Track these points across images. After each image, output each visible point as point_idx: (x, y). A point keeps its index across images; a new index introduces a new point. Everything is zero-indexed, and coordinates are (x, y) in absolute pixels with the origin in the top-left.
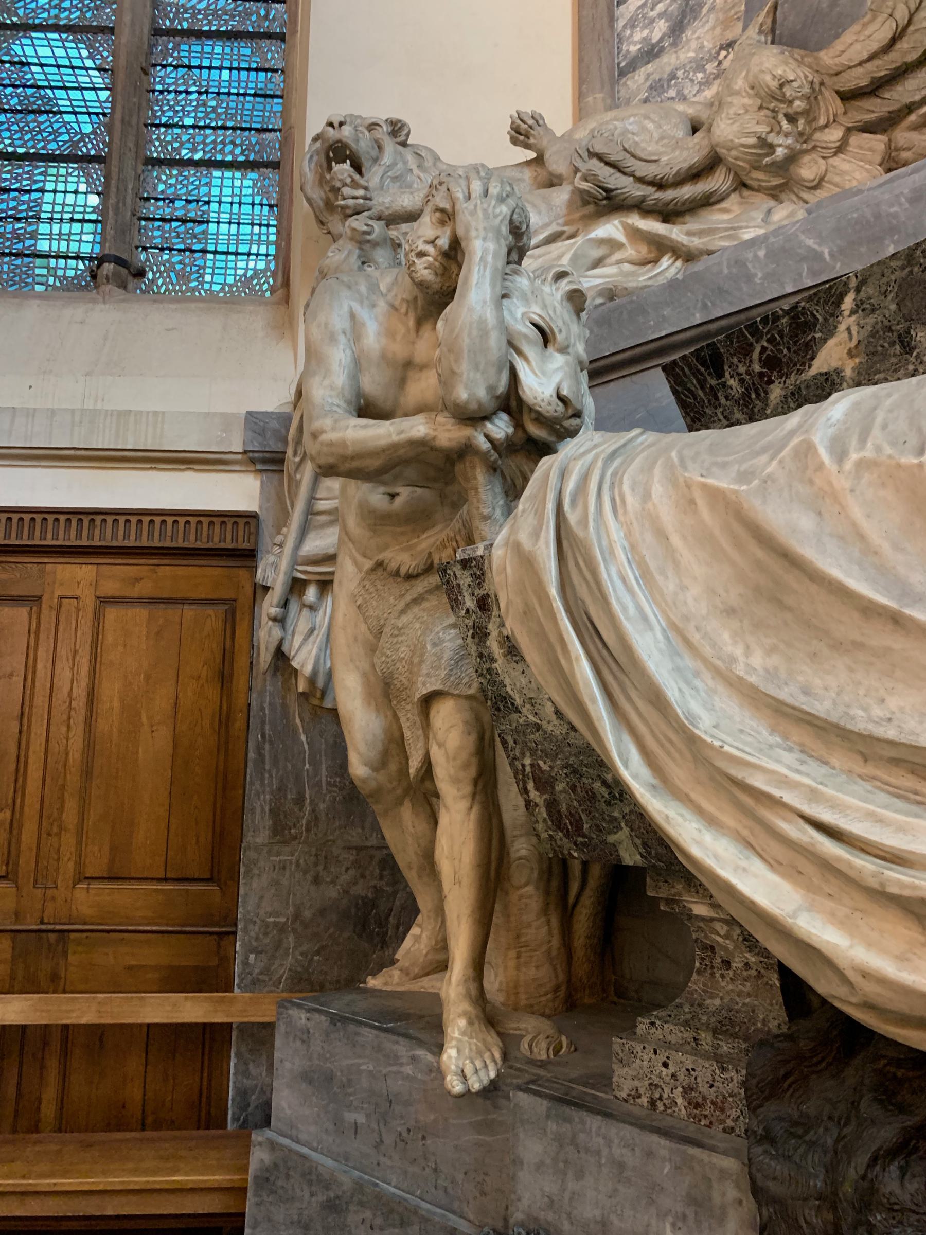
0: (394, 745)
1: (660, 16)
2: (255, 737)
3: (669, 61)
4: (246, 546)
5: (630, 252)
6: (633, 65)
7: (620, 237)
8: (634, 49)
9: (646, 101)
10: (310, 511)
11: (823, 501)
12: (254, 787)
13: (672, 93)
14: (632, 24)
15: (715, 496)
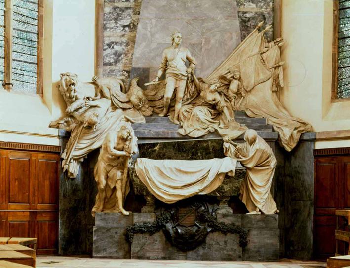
0: (107, 184)
1: (113, 58)
2: (60, 182)
3: (113, 67)
4: (58, 151)
5: (125, 119)
6: (106, 64)
7: (123, 117)
8: (107, 61)
9: (109, 73)
10: (75, 149)
11: (166, 169)
12: (60, 190)
13: (114, 74)
14: (106, 55)
15: (157, 167)
